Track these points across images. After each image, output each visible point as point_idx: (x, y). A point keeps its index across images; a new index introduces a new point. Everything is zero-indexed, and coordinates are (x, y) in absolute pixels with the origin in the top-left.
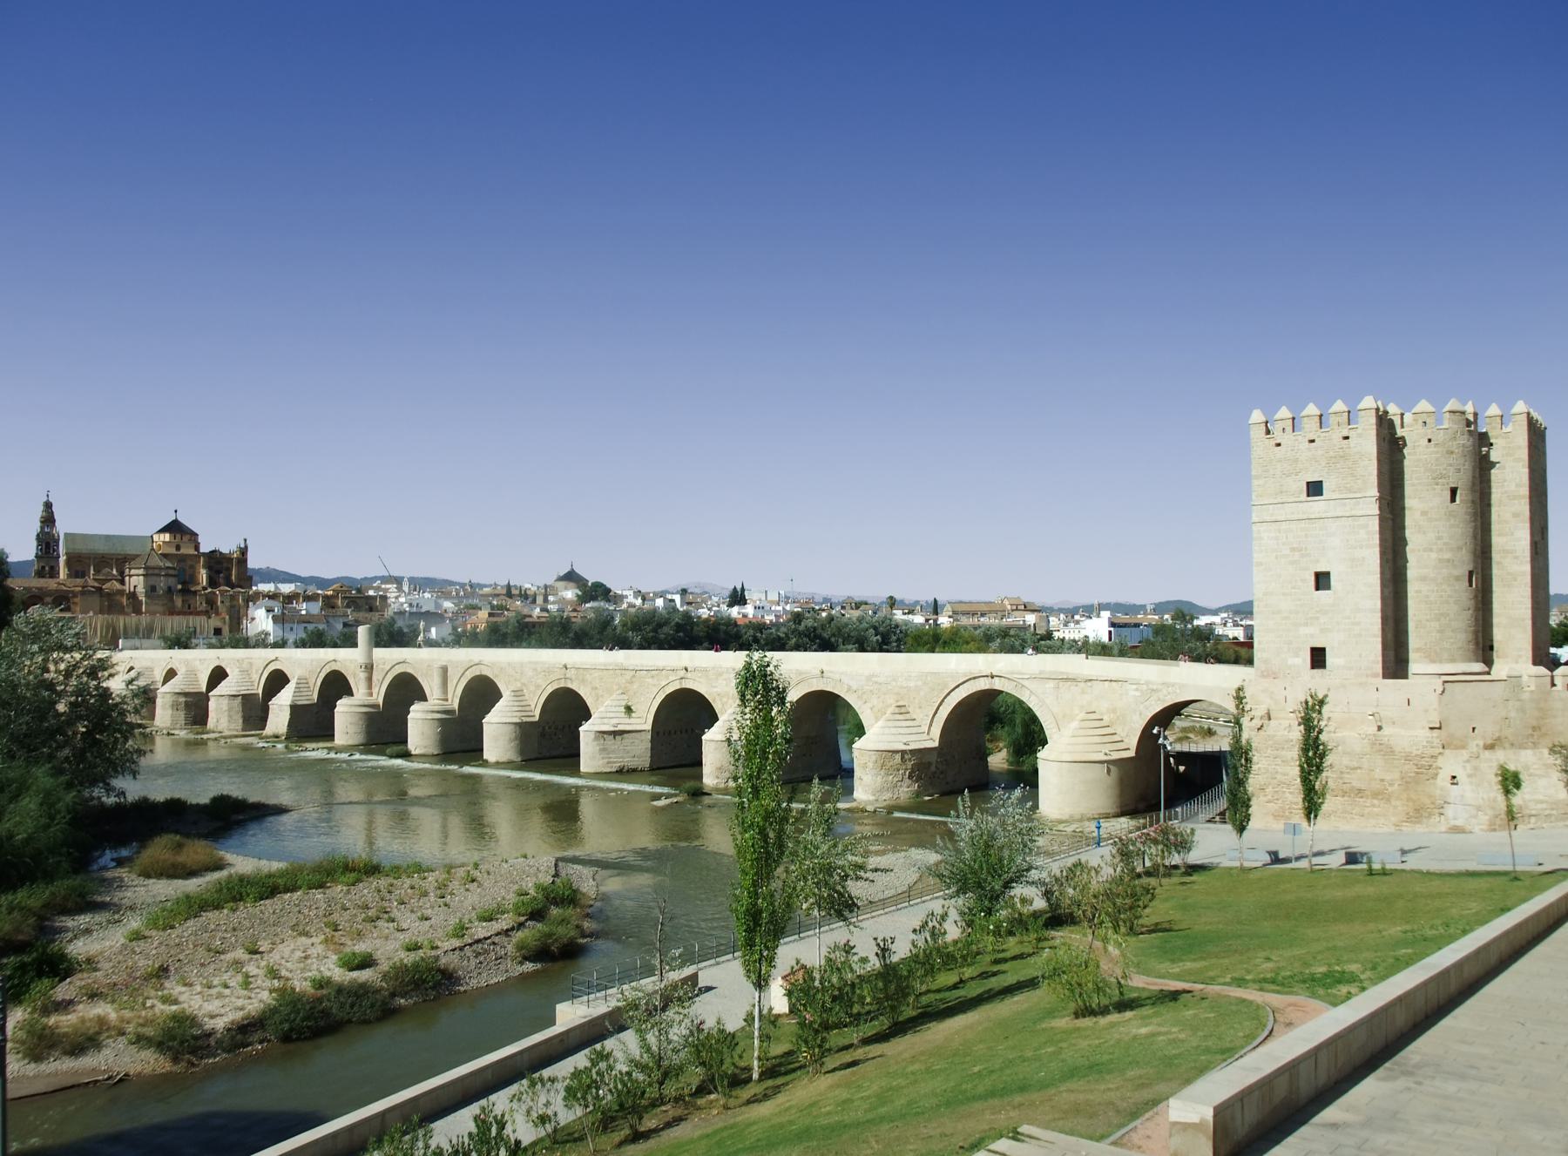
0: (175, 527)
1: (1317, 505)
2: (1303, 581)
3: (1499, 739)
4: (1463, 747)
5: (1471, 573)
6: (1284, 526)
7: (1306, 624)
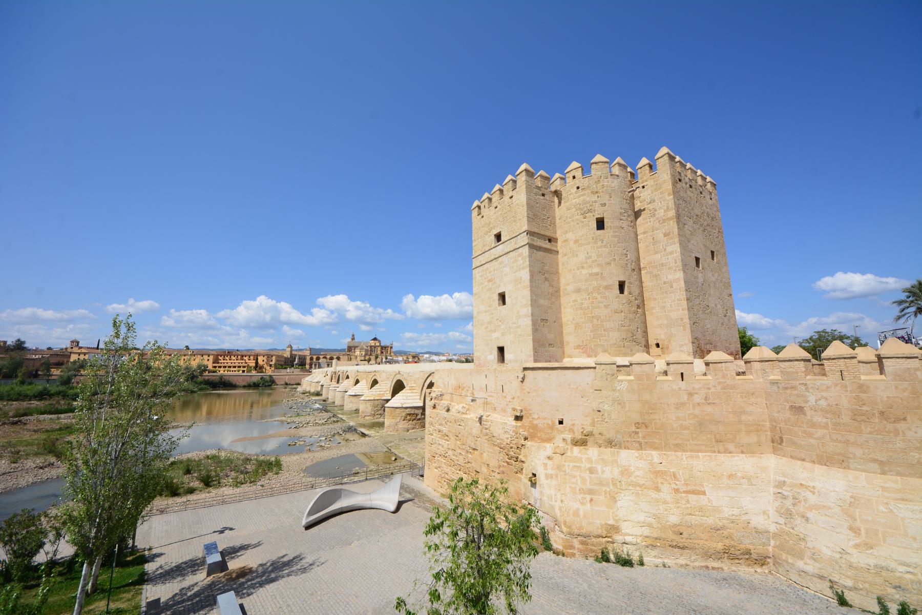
0: (375, 339)
1: (501, 249)
3: (590, 434)
5: (622, 286)
7: (495, 331)
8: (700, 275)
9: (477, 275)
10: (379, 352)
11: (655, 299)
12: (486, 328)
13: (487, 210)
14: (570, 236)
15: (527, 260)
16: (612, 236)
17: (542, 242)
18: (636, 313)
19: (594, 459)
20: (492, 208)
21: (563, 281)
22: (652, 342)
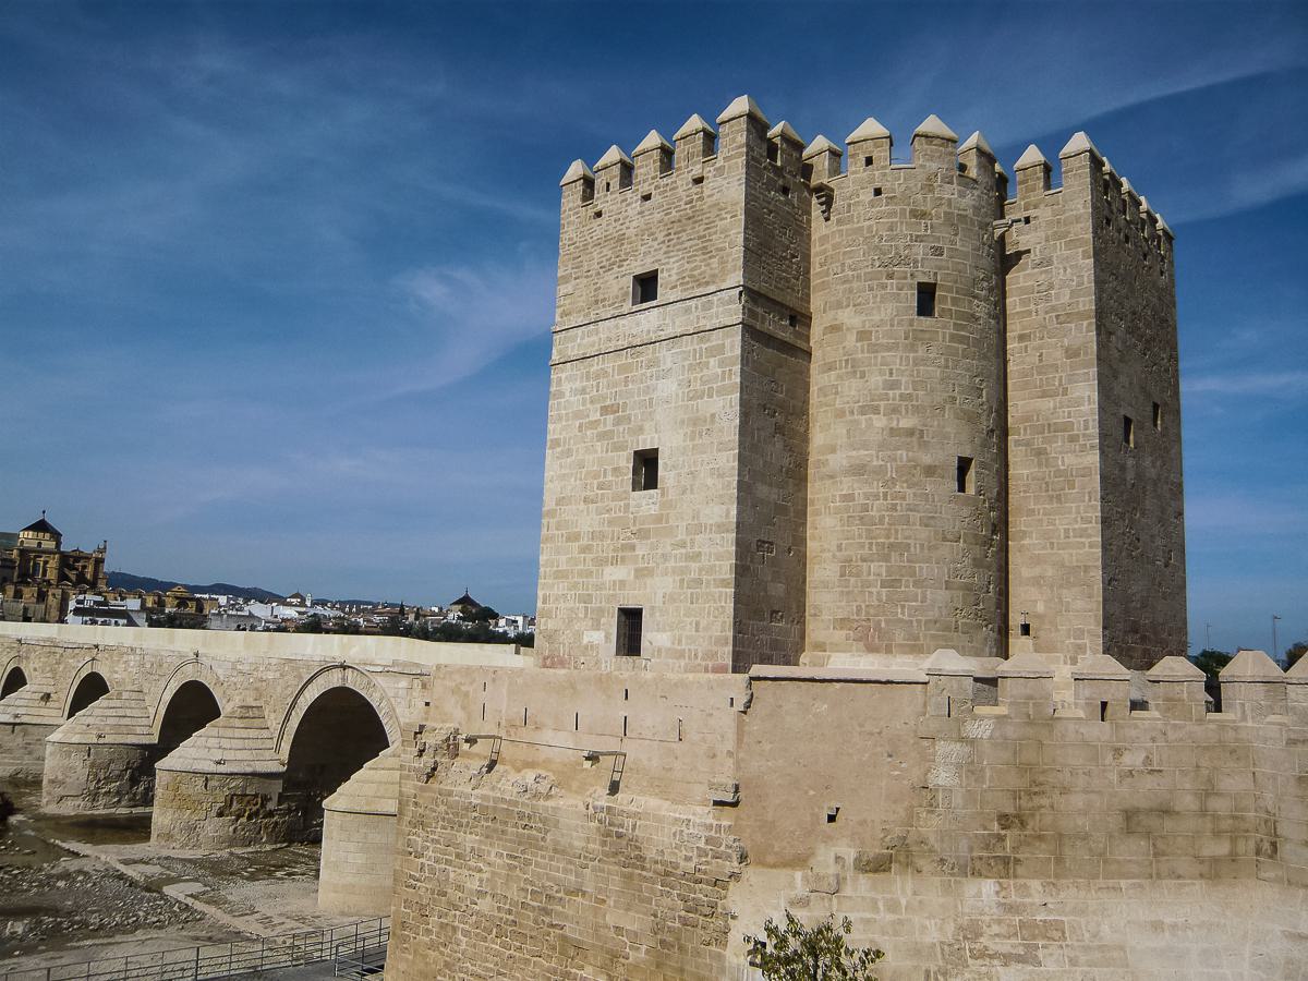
0: (41, 527)
1: (649, 320)
2: (616, 470)
4: (800, 861)
5: (964, 465)
6: (595, 365)
7: (615, 561)
8: (1130, 462)
9: (566, 387)
10: (52, 575)
11: (1031, 512)
12: (586, 549)
13: (615, 195)
14: (847, 317)
15: (737, 368)
16: (953, 338)
17: (776, 326)
18: (988, 542)
19: (904, 902)
20: (632, 195)
21: (818, 439)
22: (1015, 620)
